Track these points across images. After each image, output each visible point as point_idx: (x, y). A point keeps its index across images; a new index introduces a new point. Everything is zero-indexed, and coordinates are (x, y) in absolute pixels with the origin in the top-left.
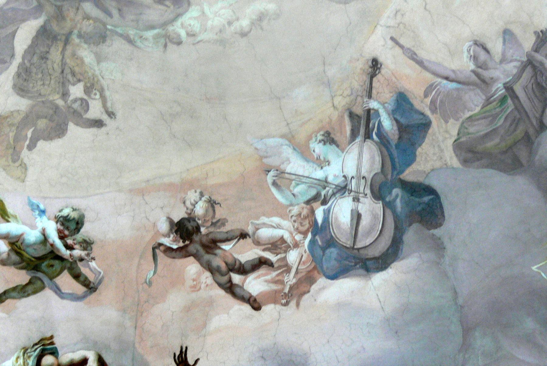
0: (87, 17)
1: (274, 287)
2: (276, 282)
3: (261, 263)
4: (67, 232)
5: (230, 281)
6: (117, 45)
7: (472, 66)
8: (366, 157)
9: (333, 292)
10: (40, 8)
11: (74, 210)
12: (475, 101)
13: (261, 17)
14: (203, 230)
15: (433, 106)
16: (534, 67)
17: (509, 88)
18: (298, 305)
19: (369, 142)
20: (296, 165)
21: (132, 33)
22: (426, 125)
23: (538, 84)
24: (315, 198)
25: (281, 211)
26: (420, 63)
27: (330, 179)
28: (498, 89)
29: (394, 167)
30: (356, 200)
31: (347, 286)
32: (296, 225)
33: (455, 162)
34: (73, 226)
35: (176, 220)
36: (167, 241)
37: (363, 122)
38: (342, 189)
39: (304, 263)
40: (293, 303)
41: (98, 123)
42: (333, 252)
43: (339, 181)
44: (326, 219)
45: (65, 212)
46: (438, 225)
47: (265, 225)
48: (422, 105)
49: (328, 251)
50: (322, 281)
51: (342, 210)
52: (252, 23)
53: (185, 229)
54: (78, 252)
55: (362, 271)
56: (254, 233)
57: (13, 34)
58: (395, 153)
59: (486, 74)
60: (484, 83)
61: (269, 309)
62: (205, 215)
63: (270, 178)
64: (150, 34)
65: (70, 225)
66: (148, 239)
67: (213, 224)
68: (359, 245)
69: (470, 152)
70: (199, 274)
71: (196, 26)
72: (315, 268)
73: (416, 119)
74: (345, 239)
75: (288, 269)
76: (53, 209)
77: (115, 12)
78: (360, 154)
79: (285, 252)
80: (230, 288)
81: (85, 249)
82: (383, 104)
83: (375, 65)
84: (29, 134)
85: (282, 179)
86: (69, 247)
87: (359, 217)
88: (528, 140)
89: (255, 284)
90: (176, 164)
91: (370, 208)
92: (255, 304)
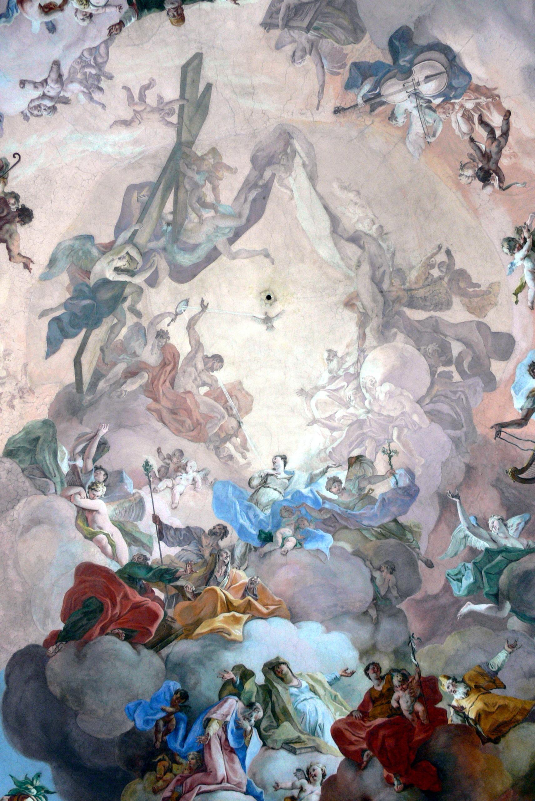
0: (392, 284)
1: (492, 108)
2: (489, 108)
3: (482, 122)
4: (517, 245)
5: (501, 136)
6: (399, 261)
7: (308, 56)
8: (391, 90)
9: (478, 72)
10: (398, 313)
11: (503, 246)
12: (327, 44)
13: (344, 188)
14: (480, 166)
15: (343, 66)
16: (288, 22)
17: (308, 29)
18: (495, 89)
19: (382, 93)
20: (417, 128)
21: (388, 256)
22: (356, 65)
23: (296, 14)
24: (430, 108)
25: (447, 124)
26: (322, 86)
27: (414, 104)
28: (312, 35)
29: (389, 71)
30: (418, 84)
32: (451, 112)
33: (367, 36)
34: (512, 243)
35: (481, 184)
36: (496, 184)
37: (373, 102)
38: (417, 95)
39: (470, 97)
40: (496, 92)
41: (448, 252)
42: (455, 83)
43: (413, 99)
45: (506, 251)
46: (407, 27)
47: (460, 130)
48: (345, 73)
49: (456, 86)
50: (475, 81)
51: (428, 89)
52: (350, 191)
53: (485, 176)
54: (526, 234)
55: (457, 60)
56: (468, 134)
57: (419, 322)
58: (380, 75)
59: (308, 47)
60: (313, 45)
61: (507, 105)
62: (472, 168)
63: (432, 140)
64: (384, 246)
65: (513, 245)
66: (501, 196)
67: (474, 161)
68: (443, 69)
69: (356, 31)
70: (506, 156)
71: (367, 222)
72: (469, 89)
73: (355, 73)
74: (444, 79)
75: (478, 105)
76: (507, 258)
77: (382, 270)
79: (469, 111)
80: (505, 134)
81: (522, 231)
82: (357, 96)
83: (337, 111)
84: (472, 290)
85: (429, 133)
86: (525, 241)
87: (427, 77)
89: (496, 120)
90: (450, 198)
91: (419, 74)
92: (507, 114)
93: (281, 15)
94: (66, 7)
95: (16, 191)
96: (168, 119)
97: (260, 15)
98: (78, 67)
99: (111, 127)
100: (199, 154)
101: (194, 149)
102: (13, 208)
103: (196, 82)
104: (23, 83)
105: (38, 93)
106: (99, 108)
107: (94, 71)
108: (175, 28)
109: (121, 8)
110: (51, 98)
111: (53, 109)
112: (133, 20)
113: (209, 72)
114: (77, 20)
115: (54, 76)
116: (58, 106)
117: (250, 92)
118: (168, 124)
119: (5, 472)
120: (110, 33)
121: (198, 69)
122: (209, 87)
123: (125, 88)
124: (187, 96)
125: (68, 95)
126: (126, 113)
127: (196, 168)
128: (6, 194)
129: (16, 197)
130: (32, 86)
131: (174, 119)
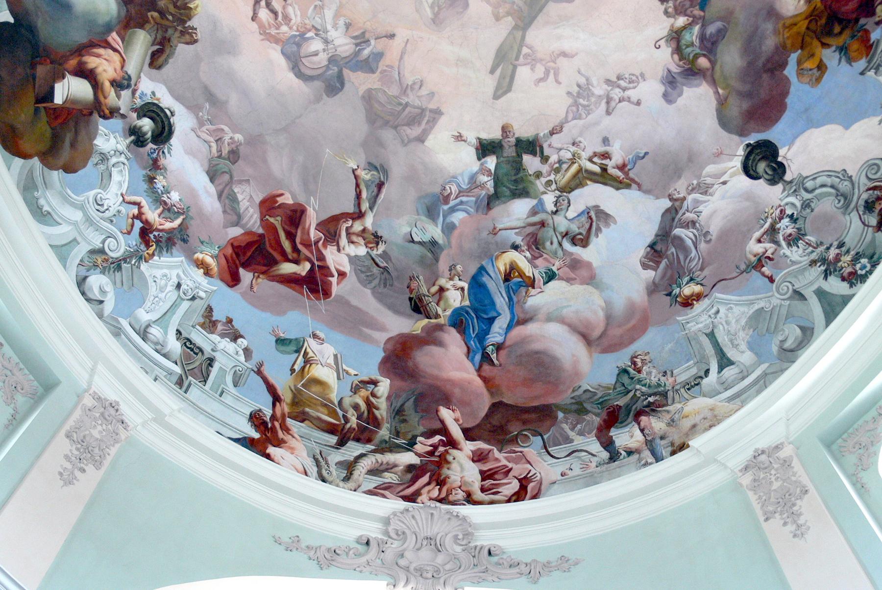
3: (275, 13)
7: (410, 84)
8: (347, 47)
9: (275, 54)
12: (394, 91)
16: (422, 113)
17: (407, 105)
18: (263, 40)
19: (354, 46)
20: (329, 14)
22: (373, 72)
23: (414, 118)
24: (316, 29)
25: (304, 14)
26: (401, 58)
27: (329, 34)
28: (404, 100)
29: (346, 63)
30: (324, 50)
31: (282, 62)
33: (361, 93)
37: (362, 40)
38: (326, 42)
40: (262, 37)
42: (295, 48)
43: (330, 39)
44: (309, 39)
48: (382, 66)
50: (279, 48)
51: (316, 45)
58: (354, 61)
60: (404, 91)
61: (254, 26)
68: (303, 60)
69: (369, 98)
74: (303, 52)
75: (277, 29)
78: (347, 44)
82: (375, 47)
83: (392, 36)
87: (317, 55)
88: (386, 123)
89: (264, 14)
91: (323, 59)
92: (254, 18)
93: (426, 119)
94: (591, 154)
95: (665, 17)
96: (529, 51)
97: (443, 121)
98: (592, 107)
99: (577, 54)
100: (510, 18)
101: (514, 23)
102: (671, 4)
103: (502, 77)
104: (638, 103)
105: (628, 93)
106: (583, 71)
107: (581, 101)
108: (510, 122)
109: (550, 145)
110: (619, 86)
111: (619, 78)
112: (542, 135)
113: (490, 83)
114: (585, 143)
115: (613, 104)
116: (614, 79)
117: (460, 62)
118: (530, 48)
120: (562, 128)
121: (497, 89)
122: (492, 72)
123: (560, 83)
124: (511, 67)
125: (606, 87)
126: (563, 62)
127: (515, 7)
128: (674, 17)
129: (666, 12)
130: (632, 100)
131: (525, 50)
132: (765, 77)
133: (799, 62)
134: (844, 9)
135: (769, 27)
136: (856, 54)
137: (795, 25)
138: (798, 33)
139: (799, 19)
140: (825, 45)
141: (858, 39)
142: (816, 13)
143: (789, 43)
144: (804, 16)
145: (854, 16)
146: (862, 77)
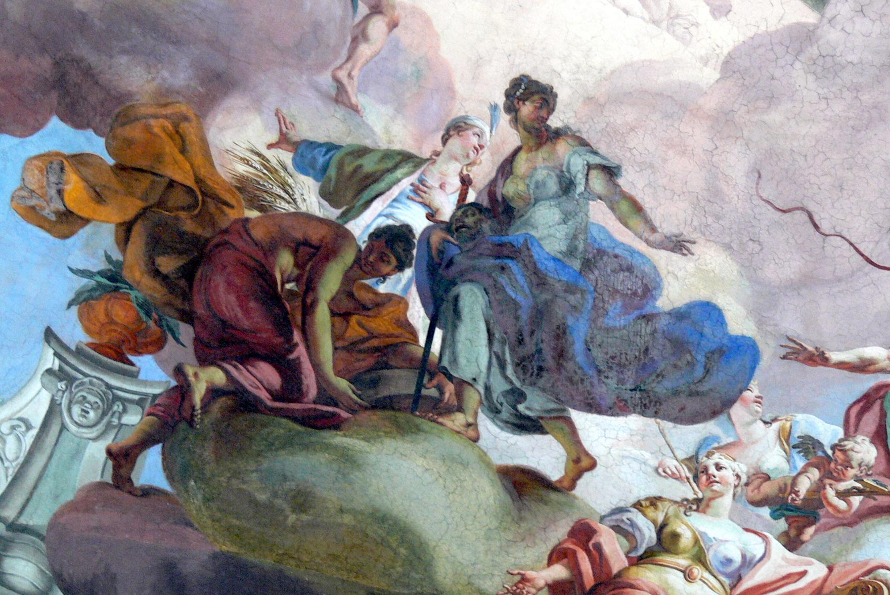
119: (859, 20)
132: (45, 63)
133: (80, 160)
134: (219, 281)
135: (180, 75)
136: (102, 318)
137: (183, 151)
138: (159, 157)
139: (199, 160)
140: (125, 231)
141: (139, 320)
142: (212, 206)
143: (134, 132)
144: (203, 172)
145: (200, 311)
146: (39, 332)
